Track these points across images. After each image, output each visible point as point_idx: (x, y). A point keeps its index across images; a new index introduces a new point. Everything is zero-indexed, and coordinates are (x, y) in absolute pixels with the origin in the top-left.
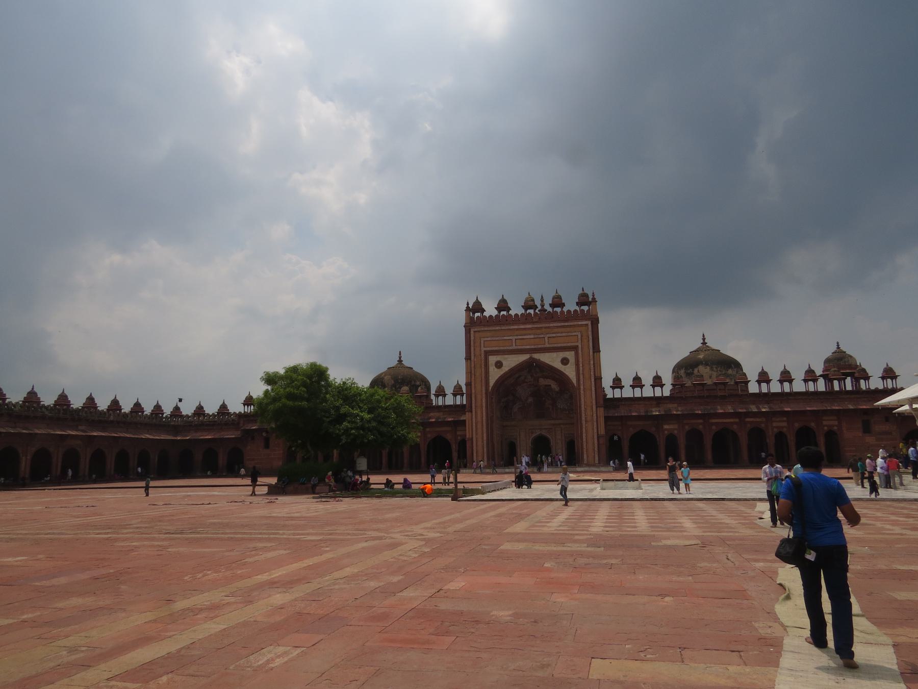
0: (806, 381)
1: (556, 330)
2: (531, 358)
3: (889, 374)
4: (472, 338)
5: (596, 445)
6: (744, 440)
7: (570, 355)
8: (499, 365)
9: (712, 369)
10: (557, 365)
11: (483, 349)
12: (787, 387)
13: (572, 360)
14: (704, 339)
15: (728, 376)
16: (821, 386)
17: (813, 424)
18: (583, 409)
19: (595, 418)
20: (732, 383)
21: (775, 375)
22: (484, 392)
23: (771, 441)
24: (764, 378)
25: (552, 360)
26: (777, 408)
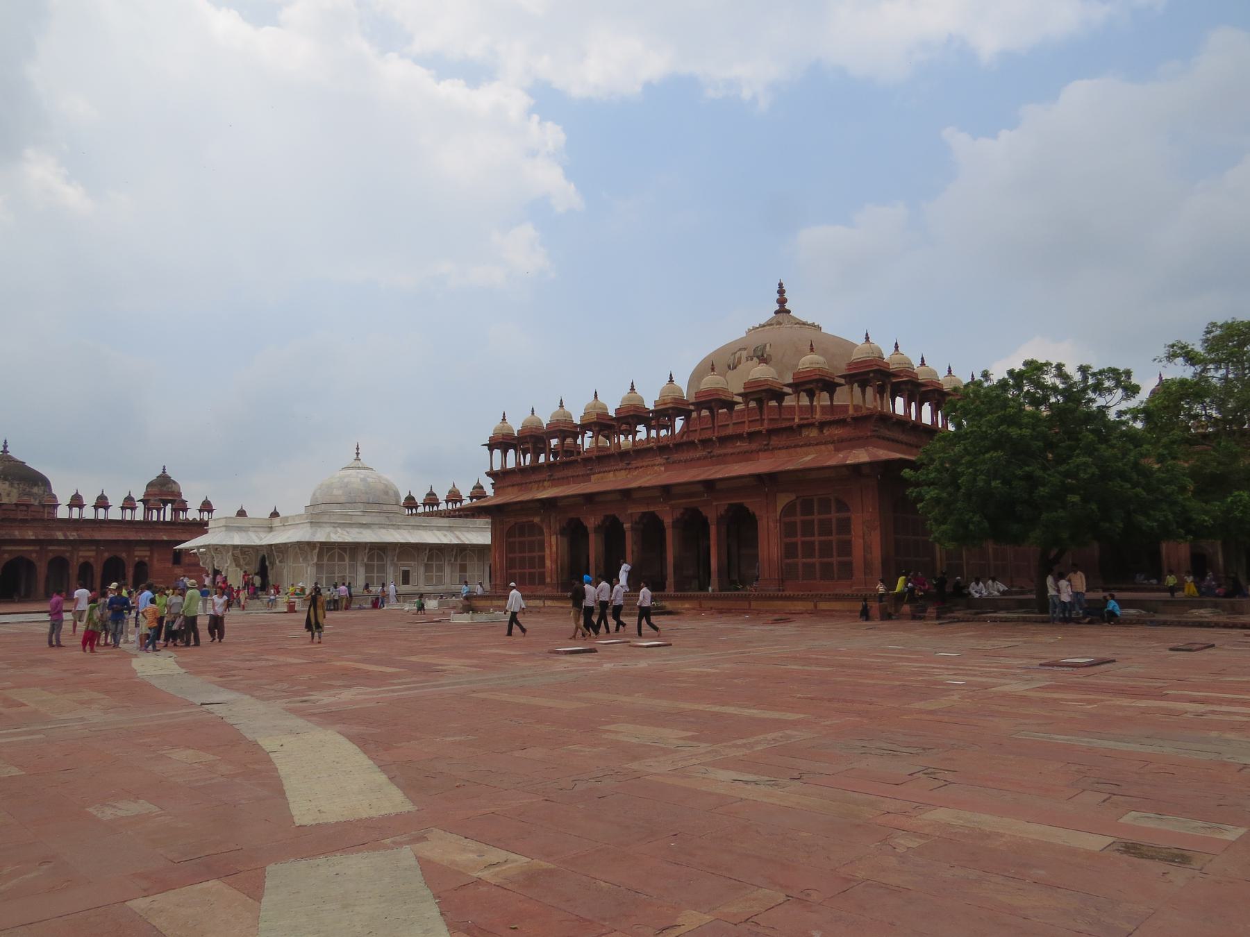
0: (123, 508)
3: (207, 507)
6: (42, 569)
9: (12, 485)
12: (101, 514)
14: (5, 447)
15: (30, 494)
16: (139, 515)
17: (124, 555)
20: (36, 503)
21: (89, 500)
23: (74, 571)
24: (77, 502)
26: (86, 535)
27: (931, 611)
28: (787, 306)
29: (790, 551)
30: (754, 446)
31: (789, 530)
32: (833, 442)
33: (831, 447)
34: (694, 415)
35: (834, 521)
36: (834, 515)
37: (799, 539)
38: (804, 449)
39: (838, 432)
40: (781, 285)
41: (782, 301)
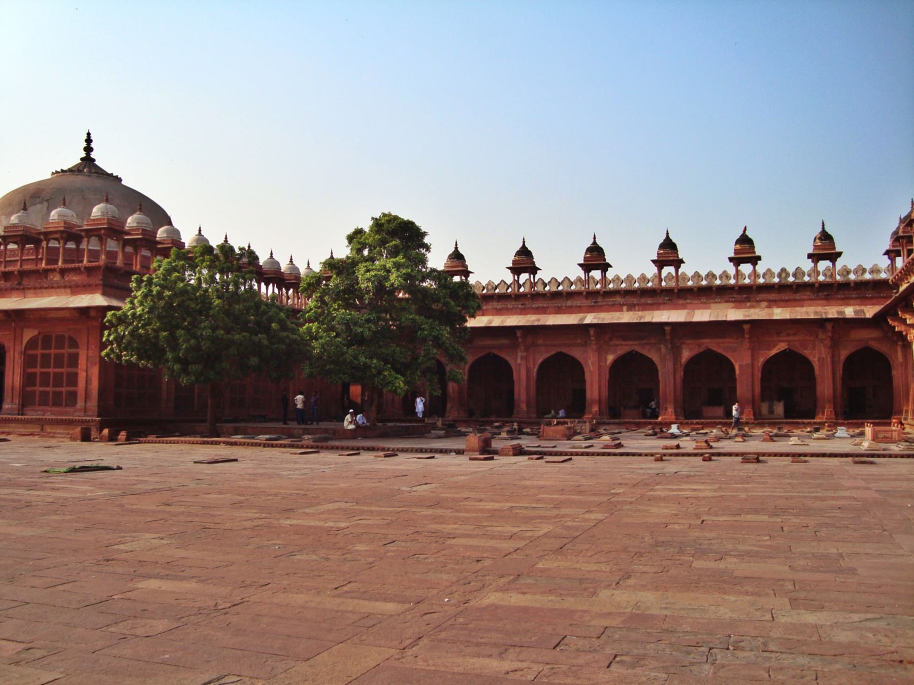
27: (123, 435)
28: (93, 155)
29: (29, 379)
30: (8, 285)
31: (29, 361)
32: (70, 287)
33: (69, 291)
34: (44, 244)
35: (66, 356)
36: (67, 351)
37: (38, 370)
38: (48, 290)
39: (75, 278)
40: (89, 134)
41: (88, 149)
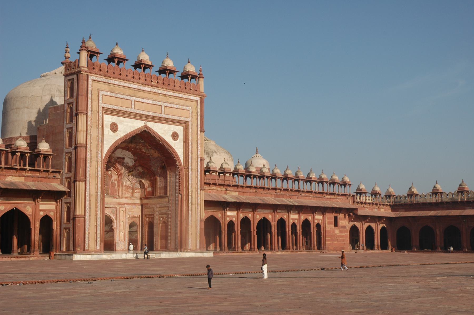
1: (172, 100)
2: (146, 126)
4: (90, 88)
5: (199, 229)
7: (180, 130)
8: (114, 127)
10: (168, 139)
11: (102, 105)
13: (181, 137)
18: (190, 191)
19: (199, 201)
22: (100, 158)
25: (163, 131)
